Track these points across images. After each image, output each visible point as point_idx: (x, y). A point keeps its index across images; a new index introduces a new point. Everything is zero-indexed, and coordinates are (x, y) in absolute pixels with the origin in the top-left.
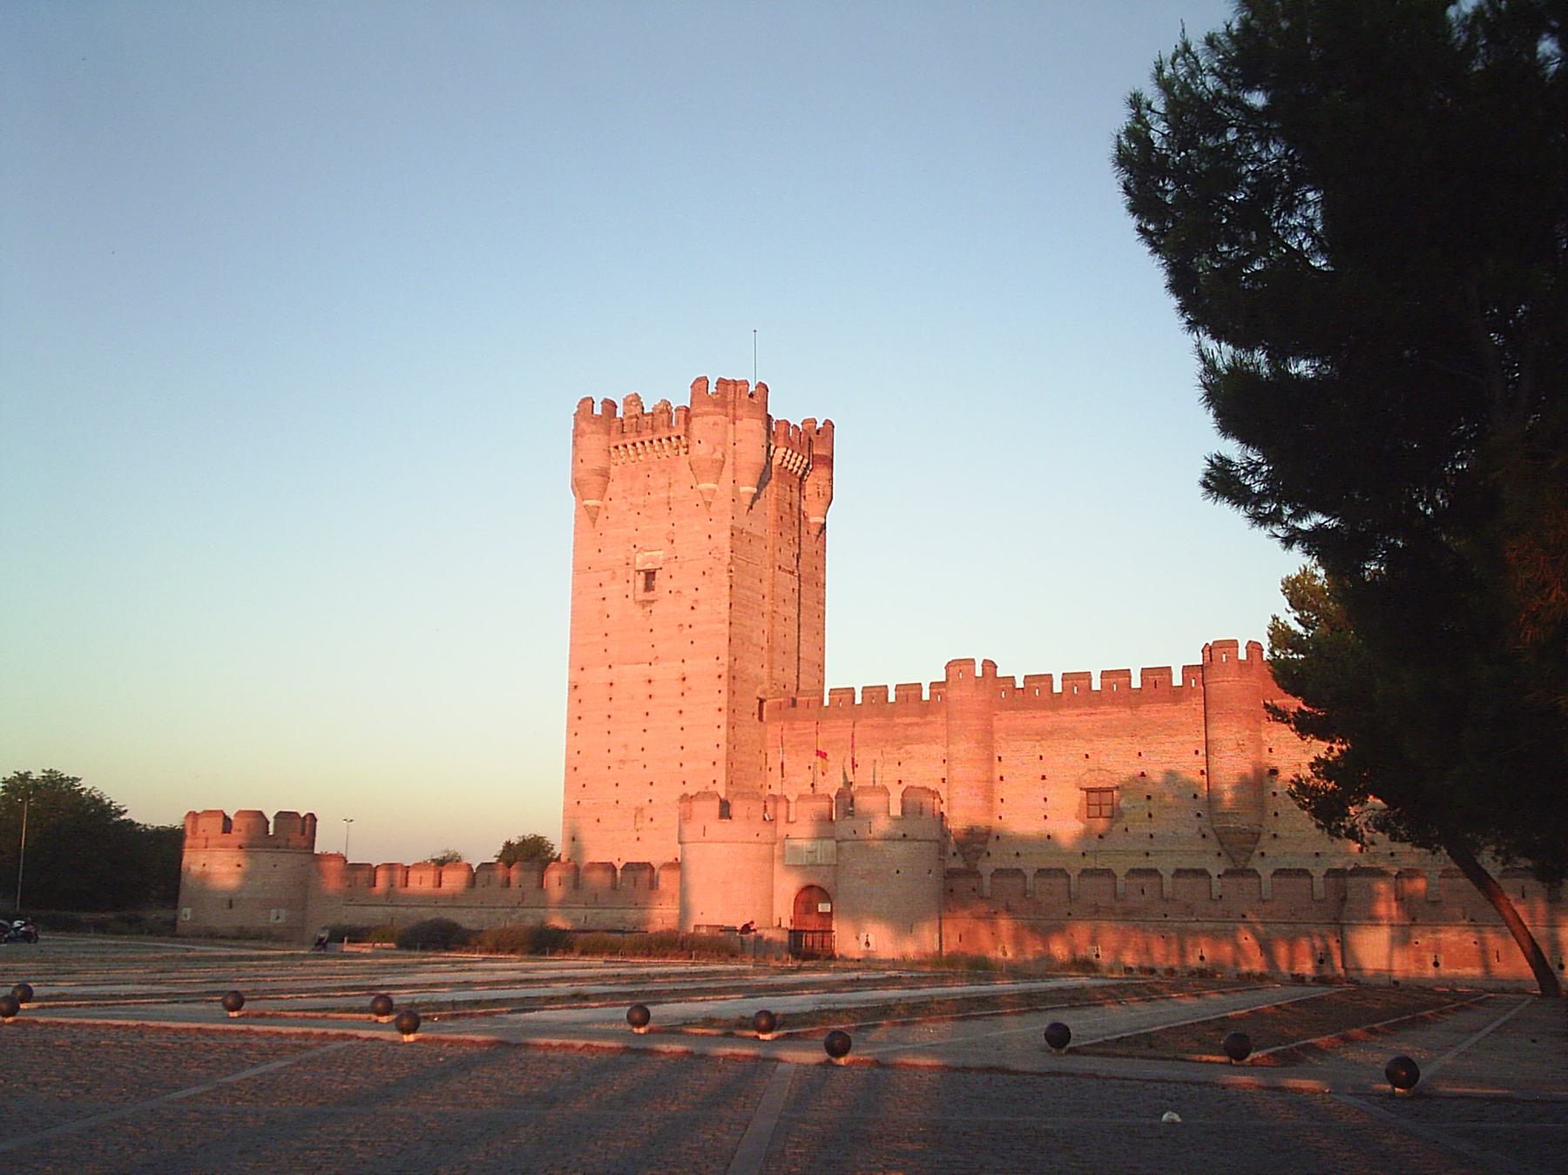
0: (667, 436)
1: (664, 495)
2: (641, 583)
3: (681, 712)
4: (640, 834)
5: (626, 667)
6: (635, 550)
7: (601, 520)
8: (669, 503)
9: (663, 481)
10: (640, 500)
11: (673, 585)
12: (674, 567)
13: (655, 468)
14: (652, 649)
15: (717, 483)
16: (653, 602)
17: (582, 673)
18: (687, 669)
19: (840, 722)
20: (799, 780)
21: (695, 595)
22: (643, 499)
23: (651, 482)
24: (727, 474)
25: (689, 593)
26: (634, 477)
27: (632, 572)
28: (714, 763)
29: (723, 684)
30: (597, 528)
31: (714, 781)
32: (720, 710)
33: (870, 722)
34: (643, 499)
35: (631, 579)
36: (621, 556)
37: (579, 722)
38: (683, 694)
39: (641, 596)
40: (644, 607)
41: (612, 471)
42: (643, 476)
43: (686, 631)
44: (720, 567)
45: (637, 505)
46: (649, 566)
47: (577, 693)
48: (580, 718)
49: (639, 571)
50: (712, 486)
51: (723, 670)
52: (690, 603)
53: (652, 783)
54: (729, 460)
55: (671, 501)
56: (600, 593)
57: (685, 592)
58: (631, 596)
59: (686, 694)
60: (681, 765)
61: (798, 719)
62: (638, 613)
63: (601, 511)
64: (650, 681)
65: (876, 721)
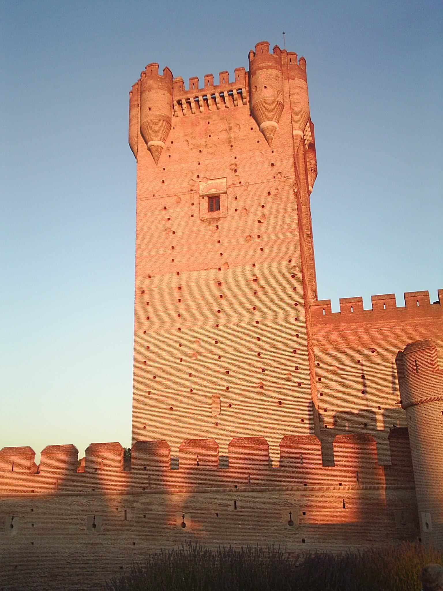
0: (229, 88)
1: (224, 136)
2: (204, 204)
3: (254, 308)
4: (218, 420)
5: (195, 274)
6: (198, 180)
7: (164, 157)
8: (230, 142)
9: (222, 126)
10: (202, 141)
11: (238, 204)
12: (238, 191)
13: (215, 117)
14: (221, 257)
15: (278, 123)
16: (219, 219)
17: (149, 281)
18: (258, 271)
19: (386, 323)
20: (350, 373)
21: (263, 211)
22: (204, 140)
23: (211, 127)
24: (286, 117)
25: (256, 212)
26: (194, 125)
27: (196, 197)
28: (295, 352)
29: (297, 283)
30: (159, 165)
31: (297, 368)
32: (296, 304)
33: (416, 321)
34: (204, 140)
35: (196, 202)
36: (185, 184)
37: (148, 321)
38: (255, 293)
39: (206, 215)
40: (210, 224)
41: (172, 121)
42: (203, 123)
43: (255, 240)
44: (286, 188)
45: (198, 146)
46: (213, 191)
47: (145, 298)
48: (148, 318)
49: (203, 197)
50: (275, 124)
51: (296, 271)
52: (257, 218)
53: (228, 372)
54: (287, 106)
55: (233, 140)
56: (166, 214)
57: (251, 209)
58: (196, 215)
59: (259, 293)
60: (259, 354)
61: (343, 322)
62: (206, 230)
63: (164, 151)
64: (220, 284)
65: (423, 320)
